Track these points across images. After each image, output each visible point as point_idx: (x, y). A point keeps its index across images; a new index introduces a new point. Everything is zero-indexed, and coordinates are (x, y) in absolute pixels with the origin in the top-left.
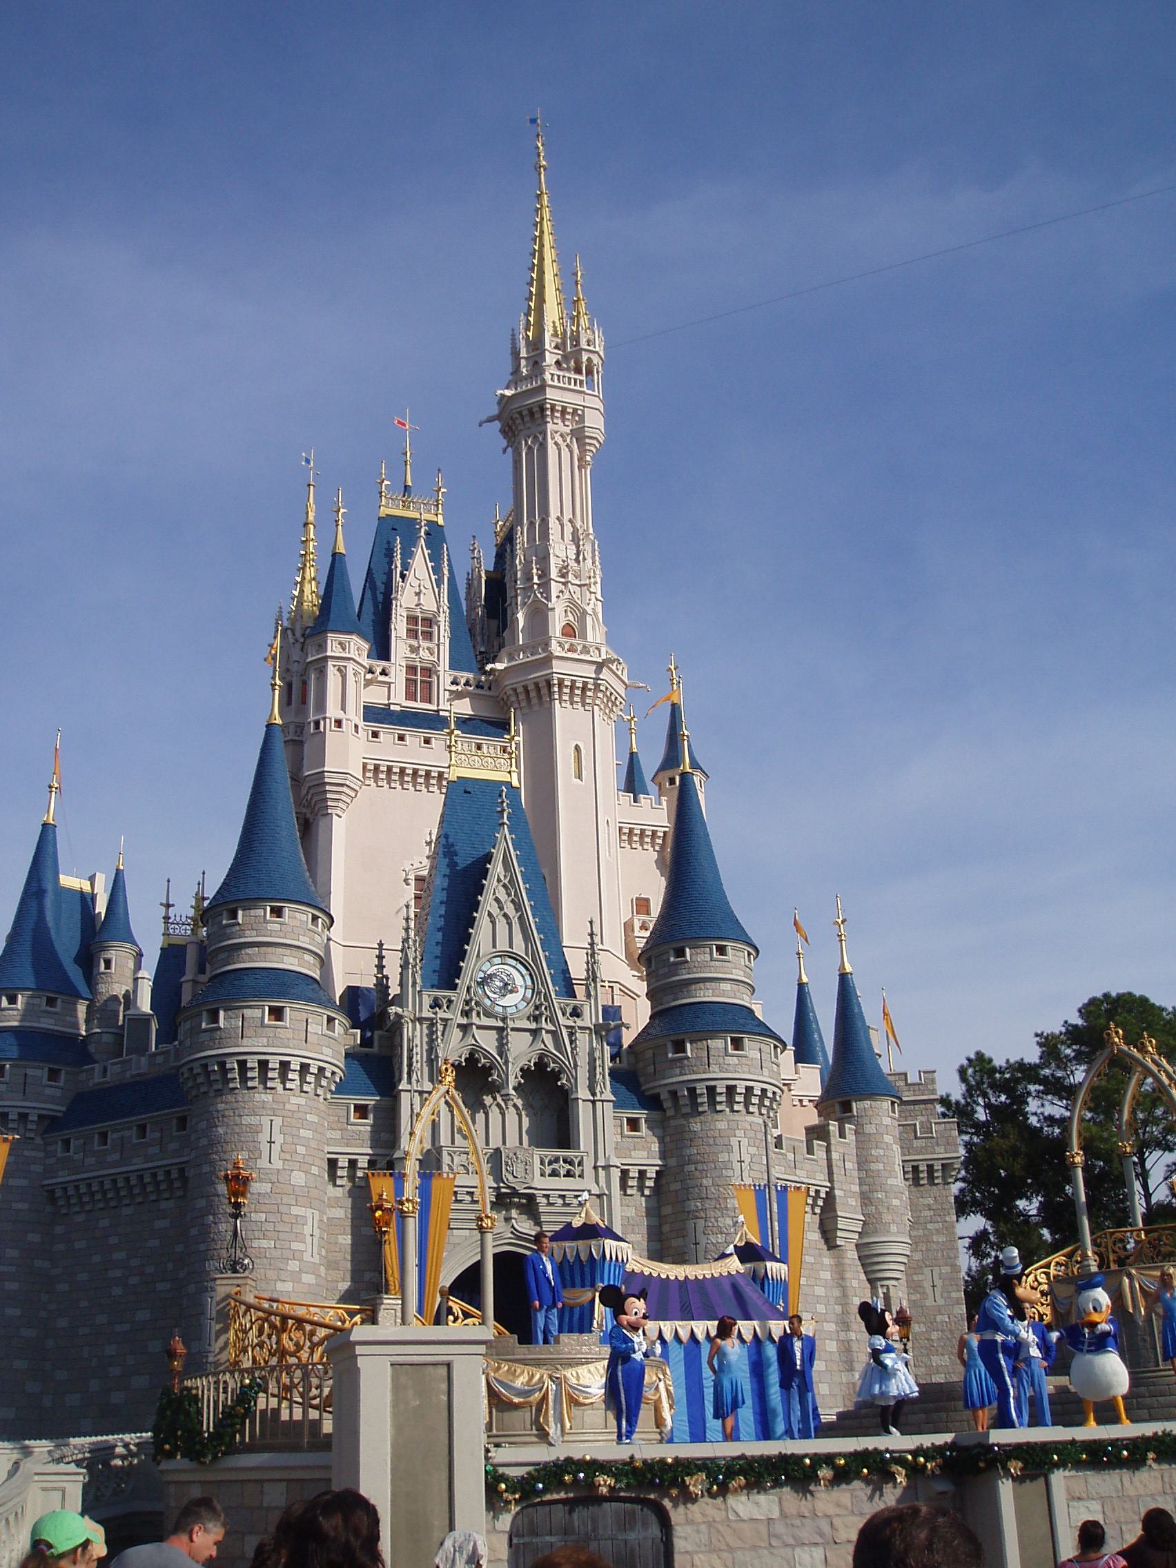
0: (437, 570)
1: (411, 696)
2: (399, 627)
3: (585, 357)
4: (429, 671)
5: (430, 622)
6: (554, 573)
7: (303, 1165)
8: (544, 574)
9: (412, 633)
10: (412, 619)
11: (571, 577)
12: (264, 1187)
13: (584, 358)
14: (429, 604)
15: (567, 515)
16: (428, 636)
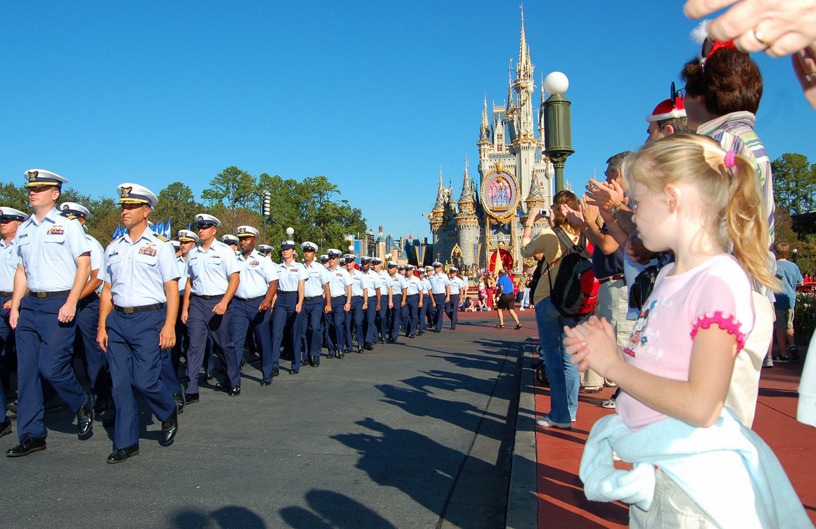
0: (502, 125)
1: (498, 150)
2: (496, 137)
3: (528, 73)
4: (501, 145)
5: (501, 135)
6: (522, 124)
7: (471, 239)
8: (520, 125)
9: (498, 138)
10: (498, 135)
11: (525, 124)
12: (466, 242)
13: (528, 75)
14: (501, 132)
15: (525, 110)
16: (501, 138)
